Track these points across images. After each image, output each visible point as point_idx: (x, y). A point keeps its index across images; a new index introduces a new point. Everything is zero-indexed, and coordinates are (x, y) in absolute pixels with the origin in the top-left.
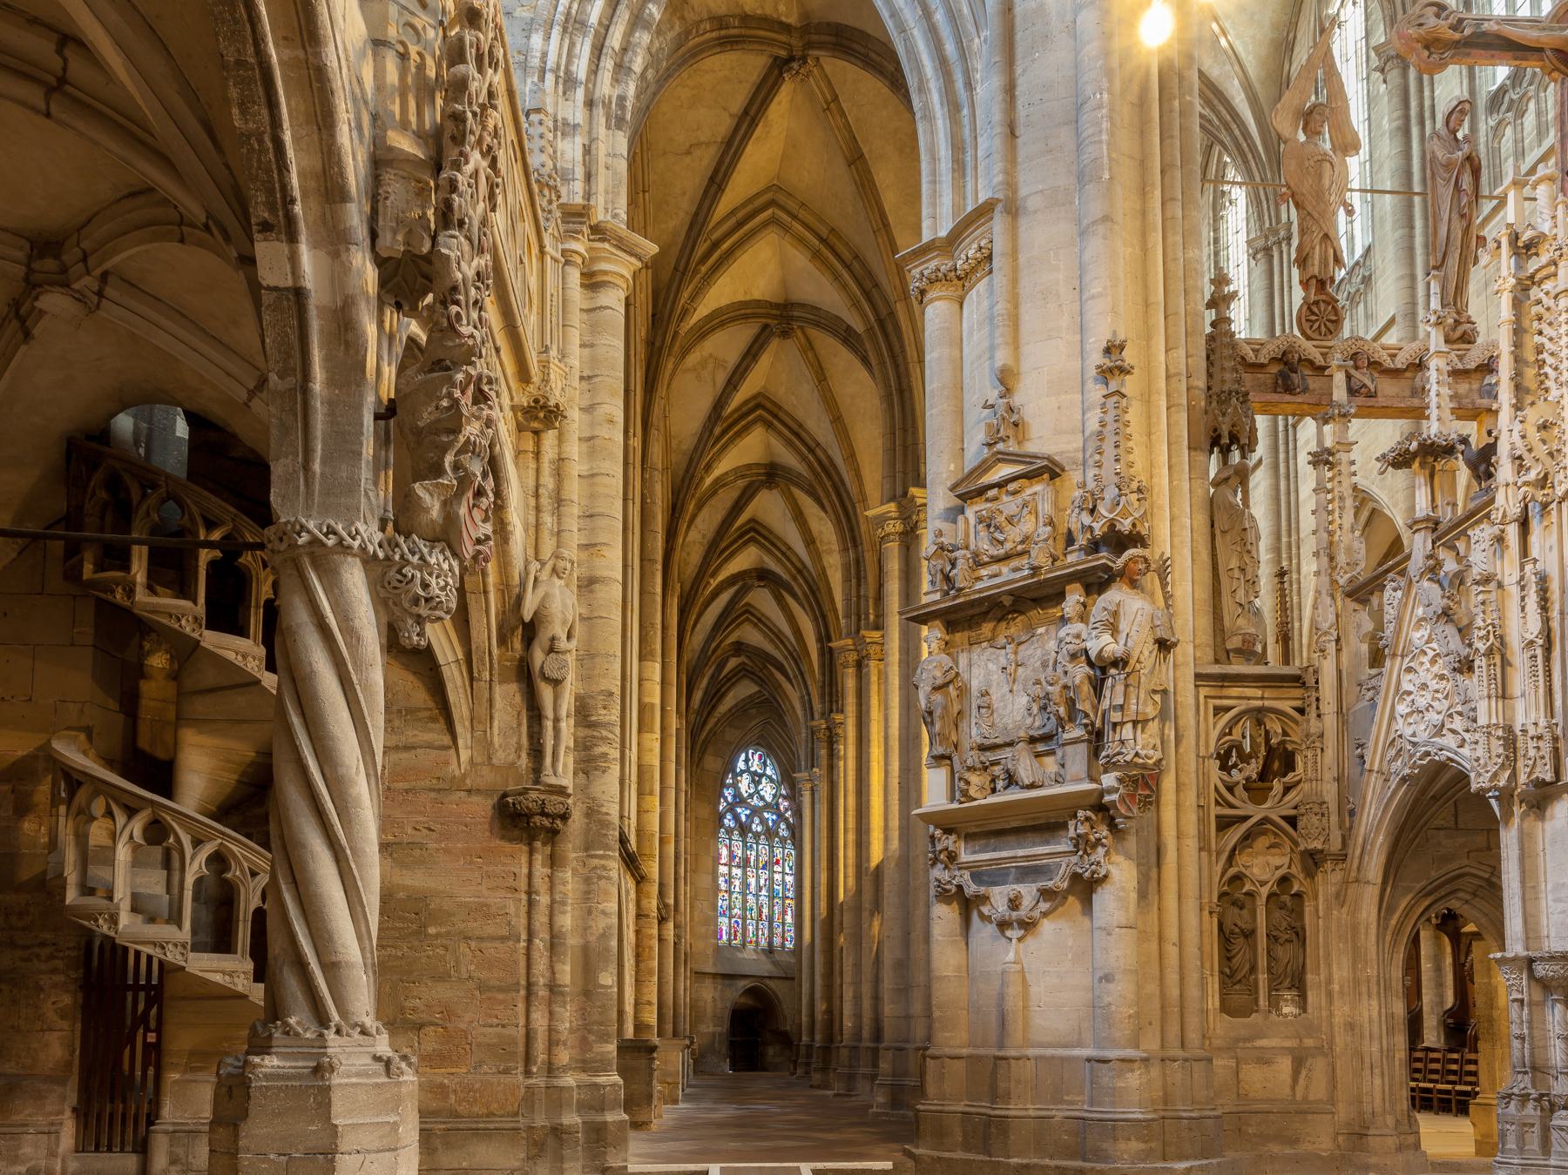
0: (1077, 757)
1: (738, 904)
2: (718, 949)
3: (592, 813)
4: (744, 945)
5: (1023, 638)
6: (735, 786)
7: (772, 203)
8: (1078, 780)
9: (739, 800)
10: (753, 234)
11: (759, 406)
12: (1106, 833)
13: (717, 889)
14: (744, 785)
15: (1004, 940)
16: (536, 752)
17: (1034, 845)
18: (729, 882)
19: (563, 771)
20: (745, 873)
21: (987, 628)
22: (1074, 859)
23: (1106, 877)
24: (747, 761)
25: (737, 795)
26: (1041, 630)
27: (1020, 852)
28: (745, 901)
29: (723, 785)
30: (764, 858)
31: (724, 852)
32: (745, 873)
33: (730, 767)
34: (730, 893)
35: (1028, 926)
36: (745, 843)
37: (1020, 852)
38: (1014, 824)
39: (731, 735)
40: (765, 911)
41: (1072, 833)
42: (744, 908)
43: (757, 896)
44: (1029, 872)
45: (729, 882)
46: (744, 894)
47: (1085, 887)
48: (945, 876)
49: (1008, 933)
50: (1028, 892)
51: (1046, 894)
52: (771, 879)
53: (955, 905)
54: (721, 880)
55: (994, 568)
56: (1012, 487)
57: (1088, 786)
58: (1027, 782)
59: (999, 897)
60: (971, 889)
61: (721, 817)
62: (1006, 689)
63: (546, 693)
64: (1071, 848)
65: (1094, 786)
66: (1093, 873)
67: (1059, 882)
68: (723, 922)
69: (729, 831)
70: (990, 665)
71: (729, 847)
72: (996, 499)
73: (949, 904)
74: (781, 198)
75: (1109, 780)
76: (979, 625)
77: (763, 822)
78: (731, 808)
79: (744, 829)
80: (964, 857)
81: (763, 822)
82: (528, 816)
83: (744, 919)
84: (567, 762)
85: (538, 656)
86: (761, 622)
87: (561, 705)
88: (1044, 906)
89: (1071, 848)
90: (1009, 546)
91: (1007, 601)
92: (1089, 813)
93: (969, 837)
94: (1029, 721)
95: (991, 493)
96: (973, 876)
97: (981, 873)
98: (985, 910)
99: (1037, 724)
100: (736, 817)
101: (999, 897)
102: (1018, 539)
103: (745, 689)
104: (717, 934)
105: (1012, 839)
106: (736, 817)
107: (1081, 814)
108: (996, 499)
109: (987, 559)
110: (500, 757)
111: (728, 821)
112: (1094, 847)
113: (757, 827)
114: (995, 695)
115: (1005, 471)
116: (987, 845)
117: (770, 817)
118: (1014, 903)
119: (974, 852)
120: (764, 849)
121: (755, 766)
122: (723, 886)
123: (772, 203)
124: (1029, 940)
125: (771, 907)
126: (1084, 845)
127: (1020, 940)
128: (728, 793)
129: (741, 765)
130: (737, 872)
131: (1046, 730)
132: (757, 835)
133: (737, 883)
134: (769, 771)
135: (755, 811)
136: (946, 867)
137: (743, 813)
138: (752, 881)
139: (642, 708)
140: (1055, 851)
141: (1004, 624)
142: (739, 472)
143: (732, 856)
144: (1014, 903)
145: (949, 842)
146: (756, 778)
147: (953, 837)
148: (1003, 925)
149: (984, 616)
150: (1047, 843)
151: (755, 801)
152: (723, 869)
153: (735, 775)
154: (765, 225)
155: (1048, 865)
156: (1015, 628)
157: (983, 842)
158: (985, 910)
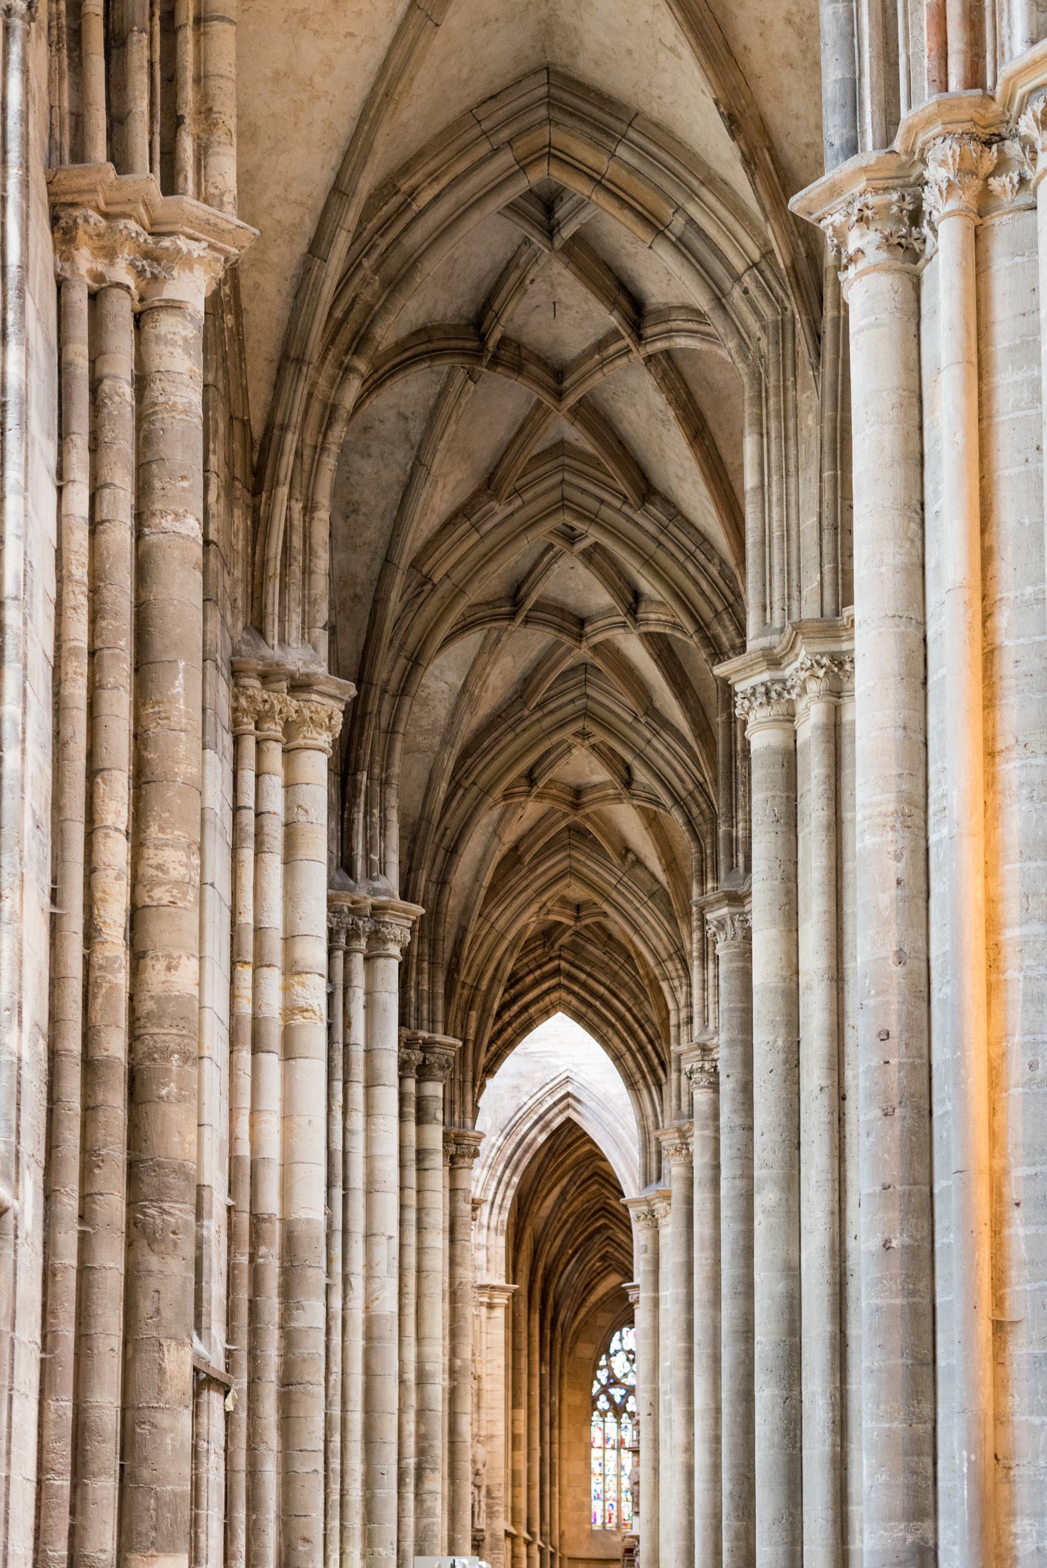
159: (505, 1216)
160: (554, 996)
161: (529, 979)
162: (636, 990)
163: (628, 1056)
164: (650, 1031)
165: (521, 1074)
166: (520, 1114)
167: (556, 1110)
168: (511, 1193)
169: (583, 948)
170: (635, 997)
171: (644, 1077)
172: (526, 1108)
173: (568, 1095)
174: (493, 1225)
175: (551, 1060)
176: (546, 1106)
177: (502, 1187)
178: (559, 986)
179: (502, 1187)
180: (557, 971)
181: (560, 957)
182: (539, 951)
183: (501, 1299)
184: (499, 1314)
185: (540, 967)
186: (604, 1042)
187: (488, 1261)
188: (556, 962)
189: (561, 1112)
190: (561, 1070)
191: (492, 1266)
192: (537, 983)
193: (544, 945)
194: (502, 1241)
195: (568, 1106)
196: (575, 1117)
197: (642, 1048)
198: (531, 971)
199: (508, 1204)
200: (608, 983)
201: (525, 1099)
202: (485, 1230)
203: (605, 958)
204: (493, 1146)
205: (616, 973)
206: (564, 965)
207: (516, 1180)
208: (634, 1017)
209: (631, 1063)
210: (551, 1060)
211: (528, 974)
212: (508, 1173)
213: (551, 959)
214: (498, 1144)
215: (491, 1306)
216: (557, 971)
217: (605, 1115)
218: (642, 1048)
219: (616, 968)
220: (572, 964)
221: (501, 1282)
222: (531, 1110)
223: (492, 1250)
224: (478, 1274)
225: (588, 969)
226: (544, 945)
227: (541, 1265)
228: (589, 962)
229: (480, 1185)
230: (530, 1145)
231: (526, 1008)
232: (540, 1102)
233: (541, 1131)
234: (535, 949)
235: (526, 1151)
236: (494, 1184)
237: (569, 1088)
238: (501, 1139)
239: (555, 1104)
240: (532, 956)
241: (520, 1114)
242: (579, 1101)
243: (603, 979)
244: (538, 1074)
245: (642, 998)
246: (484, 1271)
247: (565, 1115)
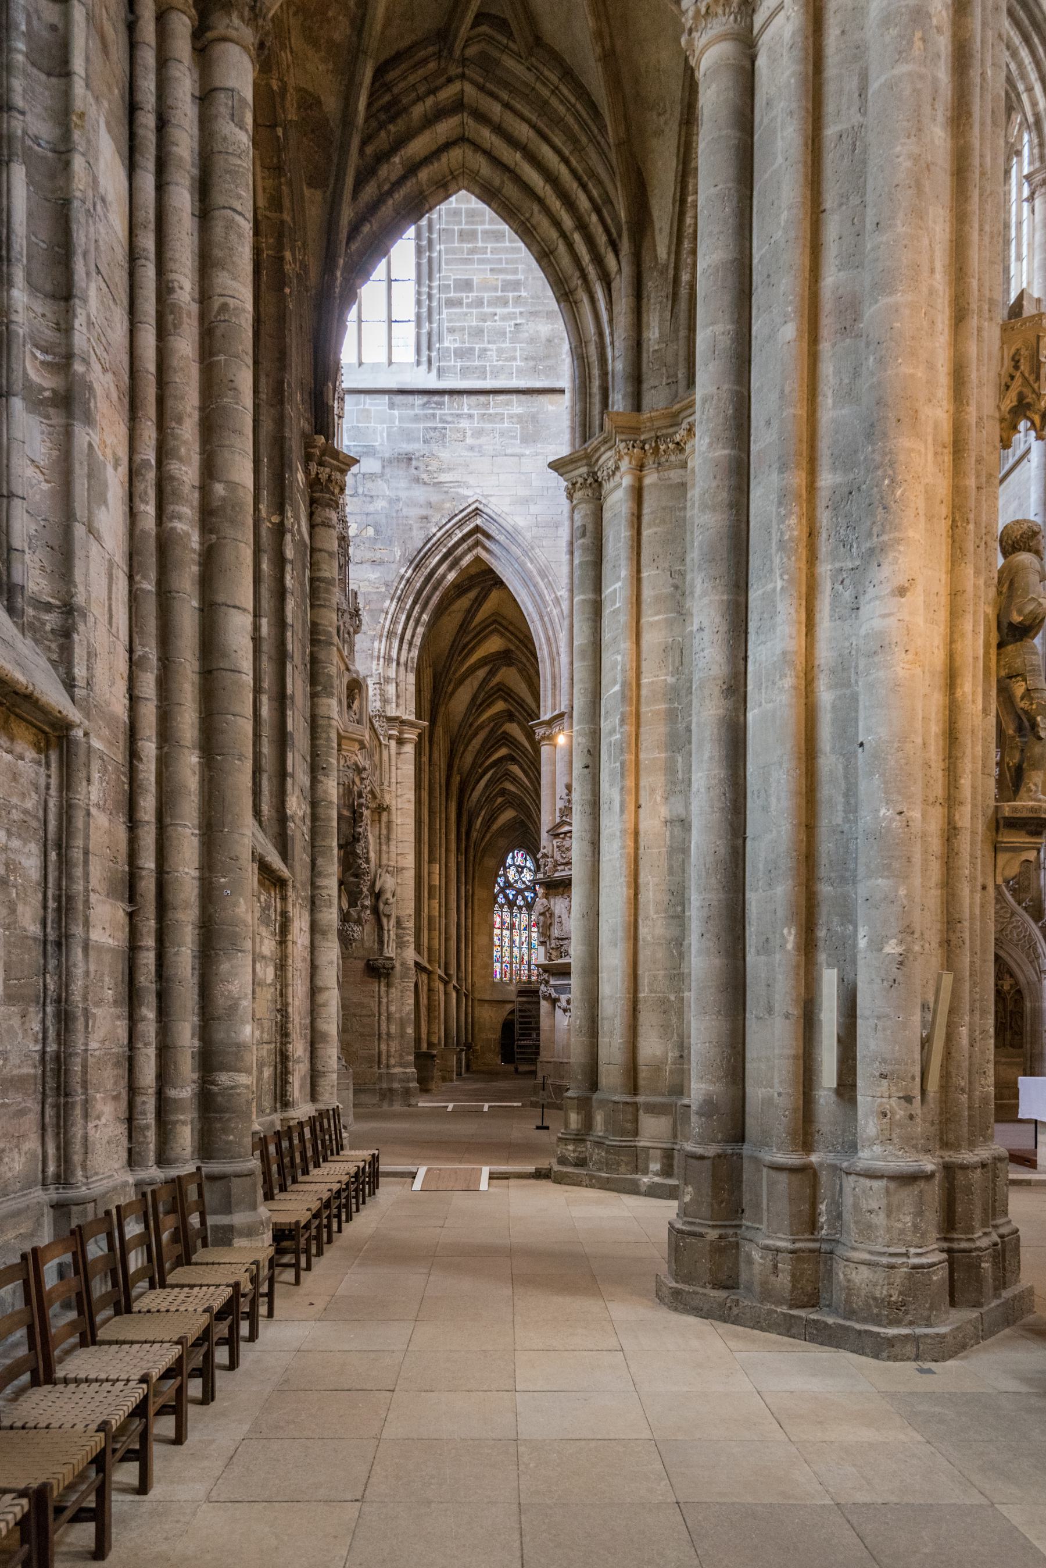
1: (508, 954)
2: (494, 984)
3: (403, 964)
4: (511, 980)
6: (505, 875)
7: (495, 621)
9: (508, 885)
10: (486, 637)
11: (499, 690)
13: (492, 943)
14: (512, 874)
16: (381, 942)
18: (501, 940)
19: (390, 951)
20: (511, 933)
24: (513, 858)
25: (507, 881)
28: (512, 952)
29: (497, 875)
30: (525, 923)
31: (498, 920)
32: (511, 933)
33: (502, 863)
34: (502, 947)
36: (512, 913)
39: (502, 842)
40: (526, 958)
42: (511, 957)
43: (520, 948)
45: (501, 940)
46: (511, 947)
52: (530, 937)
54: (496, 938)
61: (496, 896)
63: (385, 920)
68: (497, 966)
69: (501, 906)
71: (501, 917)
74: (500, 619)
77: (525, 898)
78: (502, 890)
79: (511, 904)
81: (525, 898)
82: (378, 969)
83: (511, 963)
84: (393, 945)
85: (381, 906)
86: (515, 780)
87: (390, 925)
100: (506, 896)
103: (509, 814)
104: (493, 974)
106: (506, 896)
110: (367, 945)
111: (501, 899)
113: (520, 902)
117: (529, 895)
120: (525, 917)
121: (519, 861)
122: (497, 942)
123: (495, 621)
125: (530, 955)
128: (501, 881)
129: (509, 861)
130: (506, 933)
132: (520, 908)
133: (507, 940)
134: (528, 864)
135: (520, 892)
137: (511, 893)
138: (517, 938)
139: (430, 887)
142: (491, 719)
143: (503, 923)
146: (520, 869)
151: (519, 885)
152: (497, 932)
153: (505, 868)
154: (491, 632)
159: (415, 653)
160: (456, 154)
161: (418, 111)
162: (576, 128)
163: (562, 248)
164: (595, 193)
165: (430, 505)
166: (429, 545)
167: (465, 546)
168: (420, 630)
169: (498, 63)
170: (574, 140)
171: (584, 276)
172: (435, 539)
173: (477, 529)
174: (403, 660)
175: (460, 490)
176: (455, 539)
177: (412, 622)
178: (461, 140)
179: (412, 622)
180: (458, 106)
181: (463, 76)
182: (432, 65)
183: (411, 735)
184: (409, 749)
185: (433, 92)
186: (526, 231)
187: (398, 697)
188: (454, 88)
189: (470, 549)
190: (470, 501)
191: (402, 701)
192: (429, 121)
193: (438, 55)
194: (411, 678)
195: (477, 543)
196: (484, 555)
197: (582, 226)
198: (420, 99)
199: (418, 641)
200: (534, 118)
201: (434, 530)
202: (394, 664)
203: (529, 77)
204: (402, 577)
205: (546, 103)
206: (469, 89)
207: (425, 617)
208: (573, 172)
209: (565, 260)
210: (460, 490)
211: (414, 103)
212: (417, 608)
213: (450, 80)
214: (408, 575)
215: (401, 742)
216: (458, 106)
217: (513, 548)
218: (582, 226)
219: (545, 93)
220: (481, 88)
221: (412, 718)
222: (439, 543)
223: (402, 685)
224: (388, 708)
225: (505, 96)
226: (438, 55)
227: (456, 779)
228: (506, 85)
229: (389, 617)
230: (440, 582)
231: (412, 169)
232: (449, 534)
233: (450, 569)
234: (425, 61)
235: (435, 589)
236: (404, 617)
237: (479, 521)
238: (410, 571)
239: (463, 539)
240: (421, 72)
241: (429, 545)
242: (488, 536)
243: (526, 112)
244: (448, 505)
245: (584, 140)
246: (394, 705)
247: (474, 552)
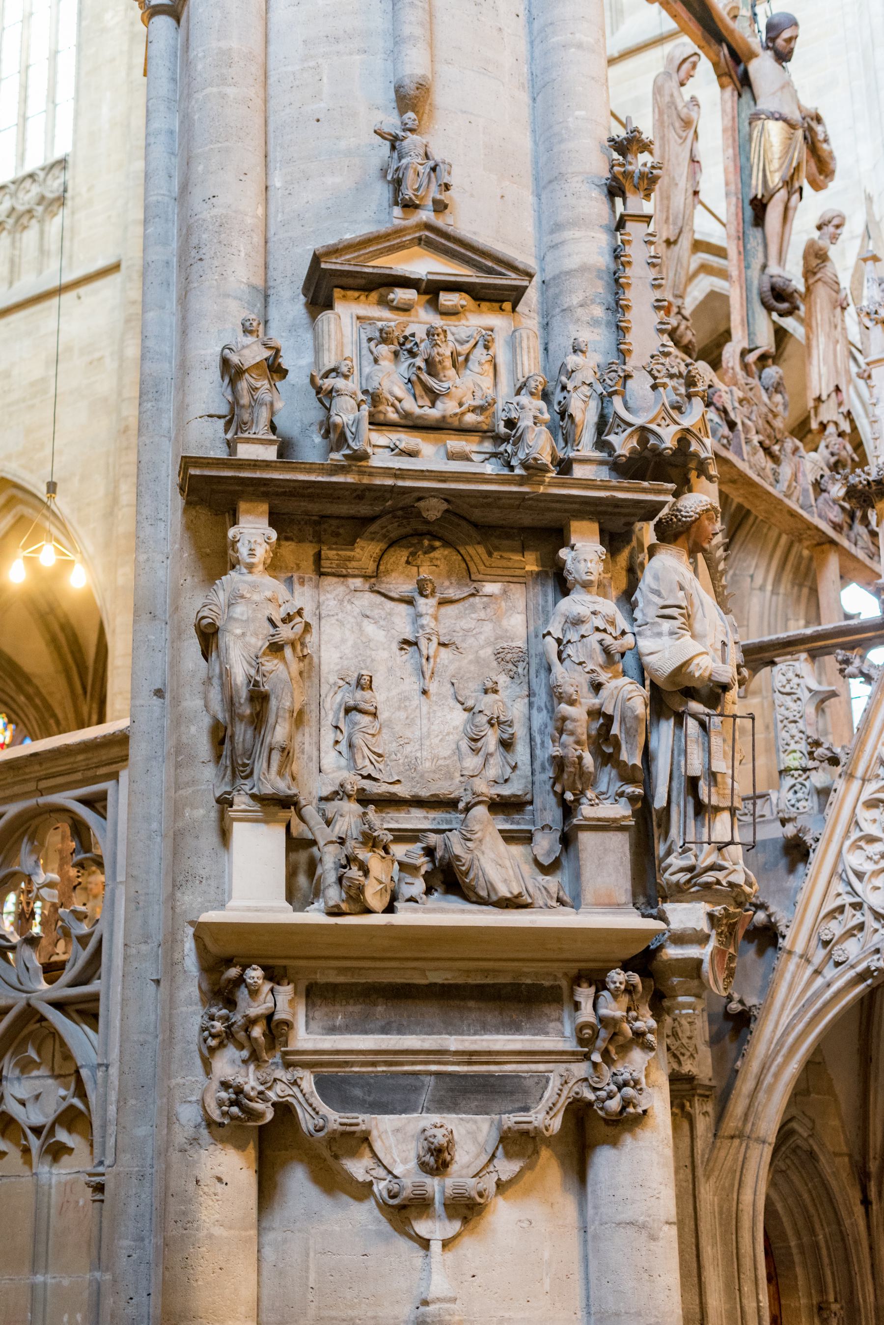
0: (606, 861)
5: (452, 593)
8: (615, 906)
12: (652, 1023)
15: (404, 1245)
17: (485, 1028)
21: (365, 552)
22: (581, 1069)
23: (645, 1112)
26: (490, 588)
27: (454, 1042)
35: (467, 1209)
37: (454, 1042)
38: (437, 978)
41: (587, 1014)
44: (468, 1090)
47: (588, 1131)
48: (250, 1080)
49: (422, 1227)
50: (470, 1134)
51: (518, 1142)
53: (251, 1152)
55: (406, 440)
56: (447, 299)
57: (632, 921)
58: (504, 891)
59: (396, 1140)
60: (318, 1114)
62: (412, 685)
64: (571, 1045)
65: (658, 925)
66: (627, 1103)
67: (545, 1116)
70: (370, 628)
72: (405, 309)
73: (240, 1147)
75: (687, 915)
76: (352, 543)
80: (306, 1038)
88: (507, 1168)
89: (571, 1045)
90: (446, 408)
91: (433, 510)
92: (636, 979)
93: (316, 994)
94: (472, 763)
95: (402, 295)
96: (321, 1083)
97: (346, 1080)
98: (358, 1168)
99: (492, 772)
101: (396, 1140)
102: (469, 402)
105: (431, 1011)
107: (618, 977)
108: (405, 309)
109: (393, 416)
112: (624, 1049)
114: (381, 696)
115: (424, 265)
116: (366, 1017)
118: (437, 1159)
119: (332, 1030)
124: (469, 1246)
126: (604, 1042)
127: (446, 1244)
131: (506, 791)
136: (255, 1058)
140: (540, 1049)
141: (402, 555)
144: (437, 1159)
145: (284, 1001)
147: (285, 992)
148: (403, 1211)
149: (357, 527)
150: (515, 1028)
155: (516, 1077)
156: (434, 566)
157: (356, 1009)
158: (358, 1168)
